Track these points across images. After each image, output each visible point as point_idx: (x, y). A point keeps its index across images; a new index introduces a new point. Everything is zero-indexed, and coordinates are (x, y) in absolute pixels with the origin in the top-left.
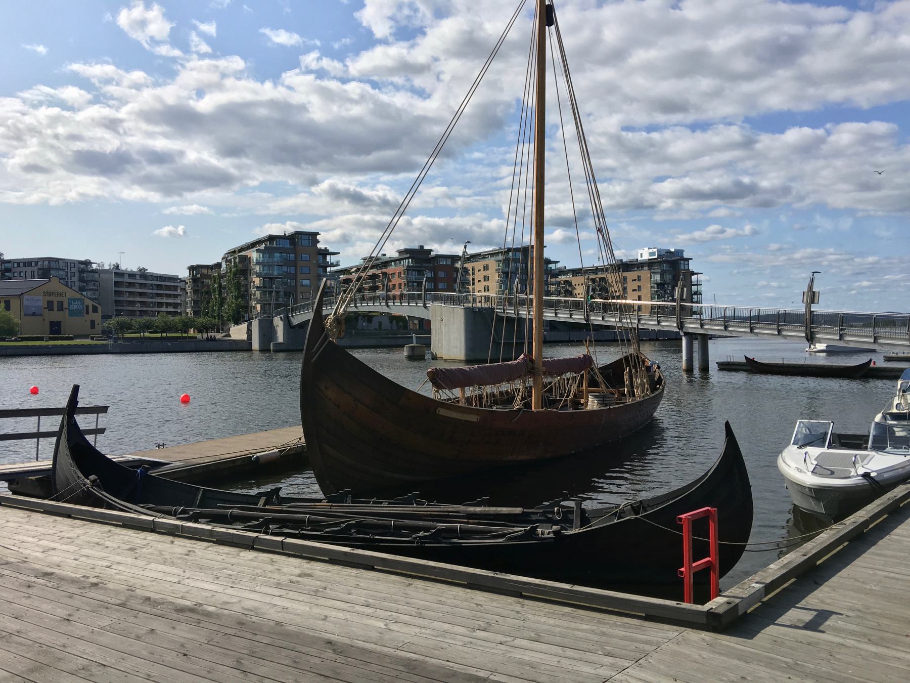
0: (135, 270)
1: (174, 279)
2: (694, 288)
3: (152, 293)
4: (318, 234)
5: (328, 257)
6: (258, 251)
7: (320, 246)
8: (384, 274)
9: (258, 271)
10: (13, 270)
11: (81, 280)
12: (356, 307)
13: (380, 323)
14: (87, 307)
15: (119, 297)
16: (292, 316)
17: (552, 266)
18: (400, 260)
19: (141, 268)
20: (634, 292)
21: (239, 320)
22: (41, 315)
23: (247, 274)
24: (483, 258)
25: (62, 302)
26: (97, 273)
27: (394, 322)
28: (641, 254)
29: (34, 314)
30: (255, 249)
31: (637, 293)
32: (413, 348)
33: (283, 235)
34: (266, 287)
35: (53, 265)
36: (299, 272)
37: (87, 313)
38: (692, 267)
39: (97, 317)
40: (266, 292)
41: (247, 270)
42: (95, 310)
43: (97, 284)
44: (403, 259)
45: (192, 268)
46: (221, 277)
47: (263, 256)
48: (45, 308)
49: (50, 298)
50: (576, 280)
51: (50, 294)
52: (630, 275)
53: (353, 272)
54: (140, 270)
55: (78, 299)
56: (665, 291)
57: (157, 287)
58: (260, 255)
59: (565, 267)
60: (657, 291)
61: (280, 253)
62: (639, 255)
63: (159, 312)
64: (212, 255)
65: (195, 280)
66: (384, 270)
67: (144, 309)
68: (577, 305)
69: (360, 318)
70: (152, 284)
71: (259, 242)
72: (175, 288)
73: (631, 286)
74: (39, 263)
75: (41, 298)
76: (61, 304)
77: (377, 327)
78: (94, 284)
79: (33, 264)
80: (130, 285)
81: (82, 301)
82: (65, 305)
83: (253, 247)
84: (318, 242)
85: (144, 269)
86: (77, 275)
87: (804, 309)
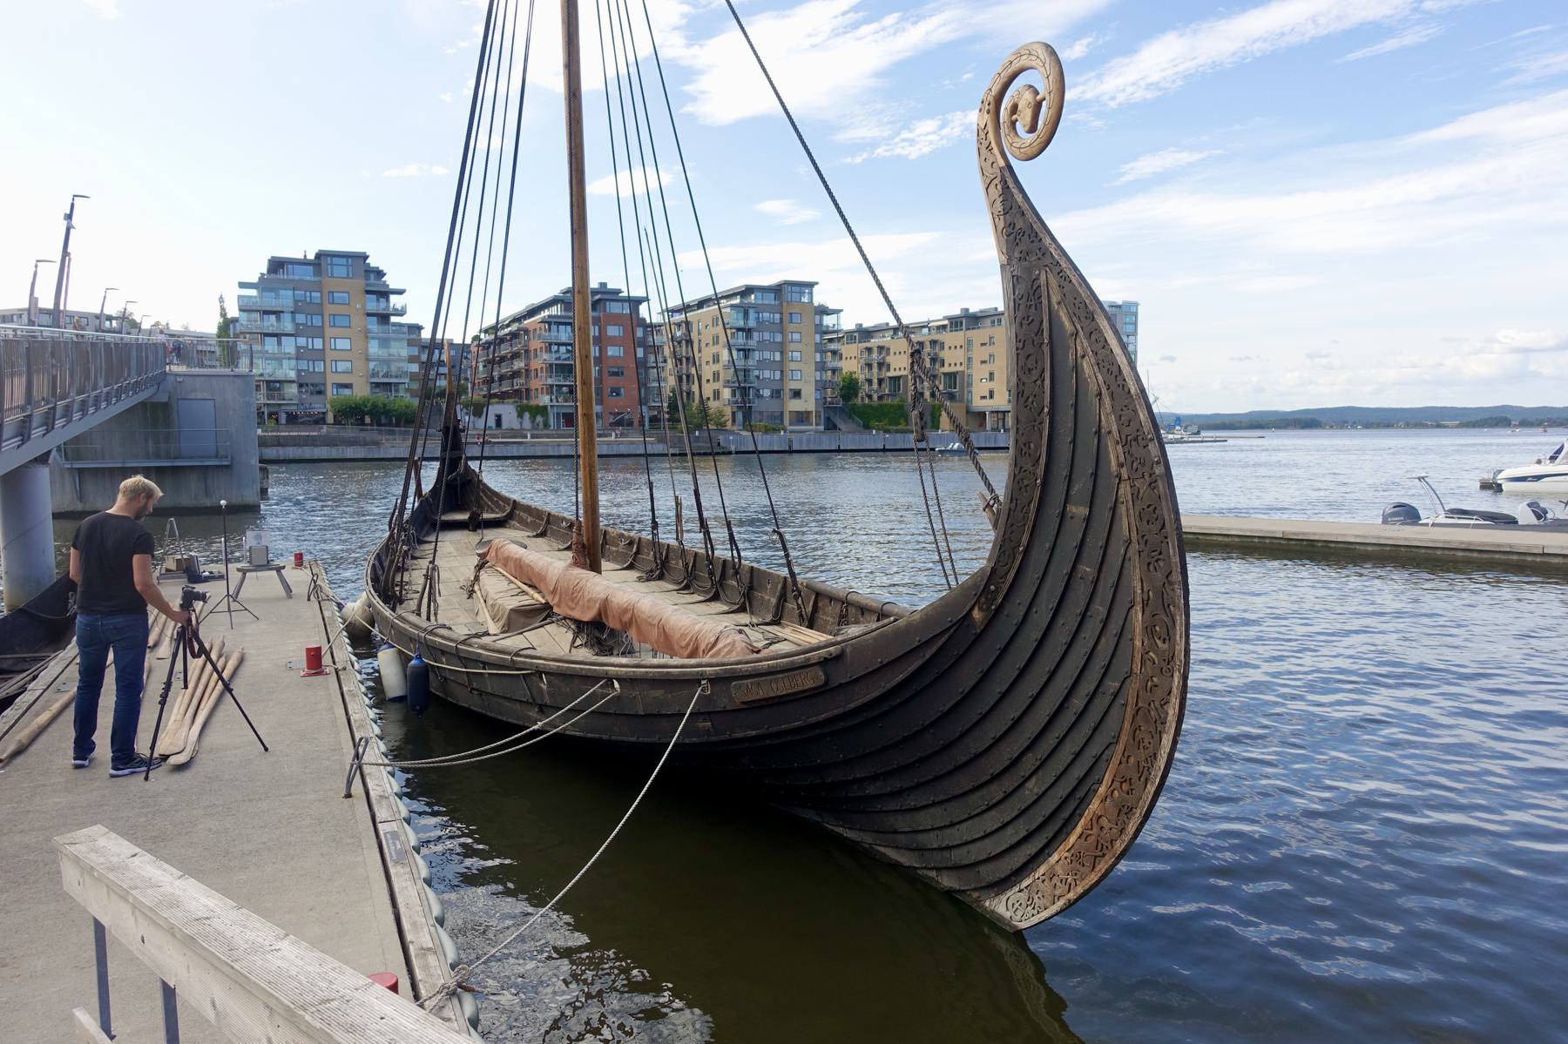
20: (984, 365)
27: (527, 415)
36: (327, 325)
52: (979, 335)
73: (979, 354)
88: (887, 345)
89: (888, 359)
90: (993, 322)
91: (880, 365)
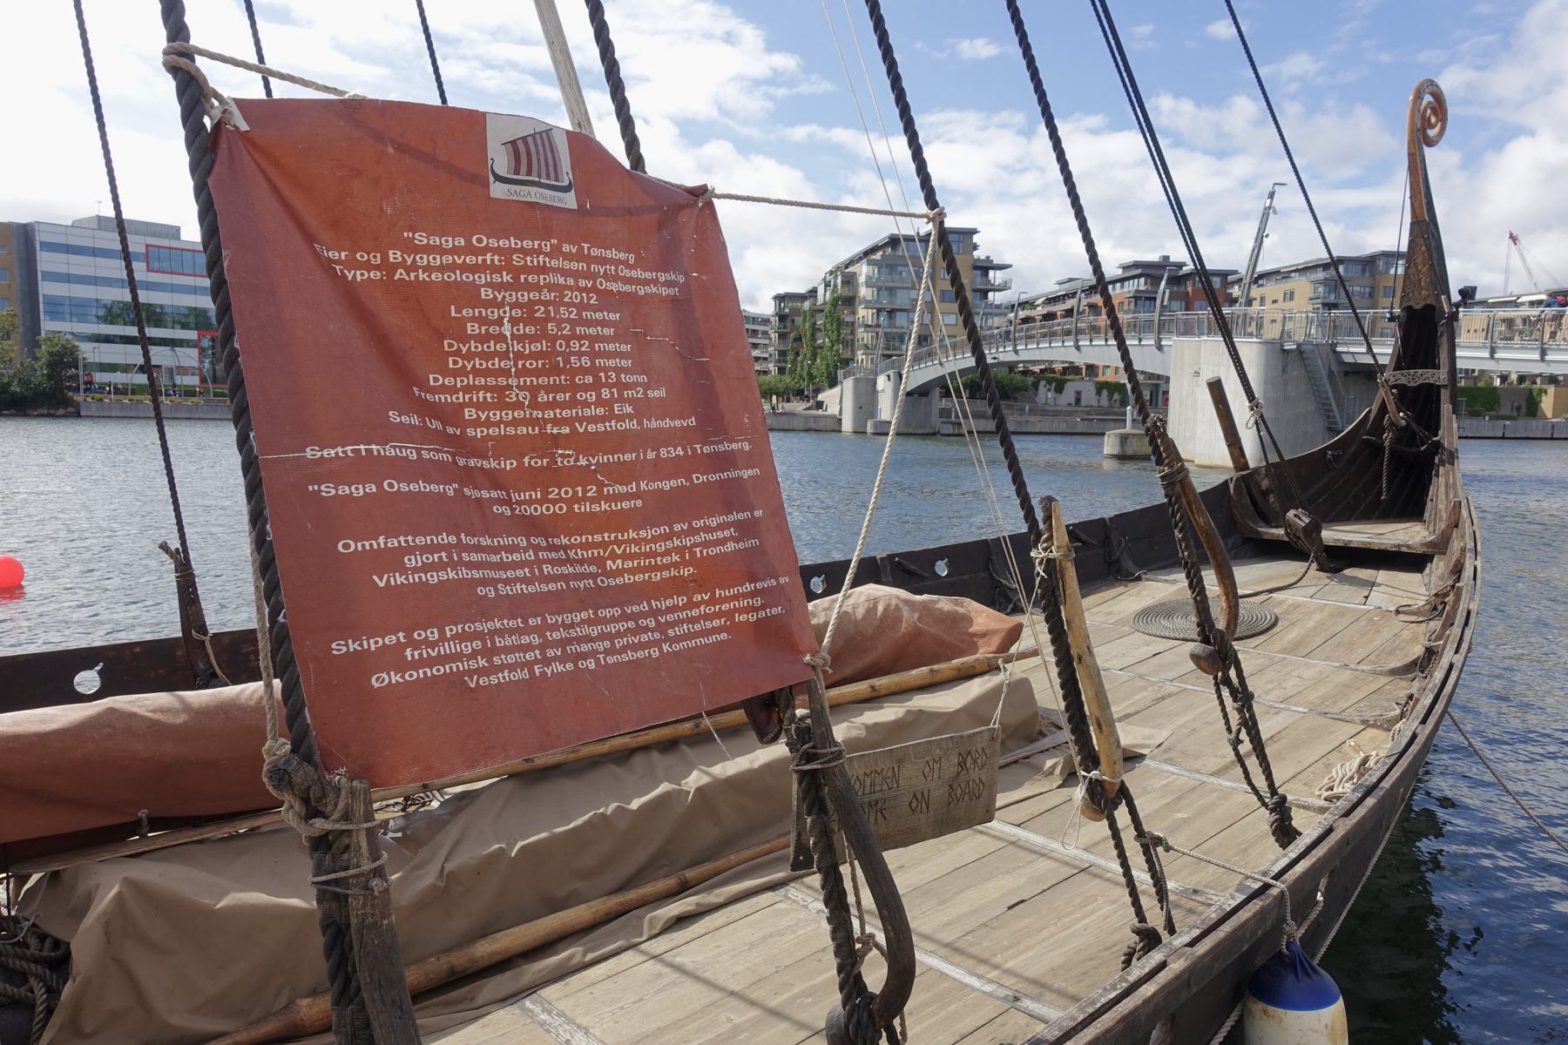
4: (974, 232)
5: (991, 273)
7: (979, 254)
13: (1079, 393)
24: (1283, 278)
27: (1105, 393)
32: (1124, 439)
44: (1128, 279)
46: (816, 311)
47: (879, 271)
53: (1038, 305)
69: (1043, 383)
71: (873, 250)
77: (1072, 401)
84: (975, 247)
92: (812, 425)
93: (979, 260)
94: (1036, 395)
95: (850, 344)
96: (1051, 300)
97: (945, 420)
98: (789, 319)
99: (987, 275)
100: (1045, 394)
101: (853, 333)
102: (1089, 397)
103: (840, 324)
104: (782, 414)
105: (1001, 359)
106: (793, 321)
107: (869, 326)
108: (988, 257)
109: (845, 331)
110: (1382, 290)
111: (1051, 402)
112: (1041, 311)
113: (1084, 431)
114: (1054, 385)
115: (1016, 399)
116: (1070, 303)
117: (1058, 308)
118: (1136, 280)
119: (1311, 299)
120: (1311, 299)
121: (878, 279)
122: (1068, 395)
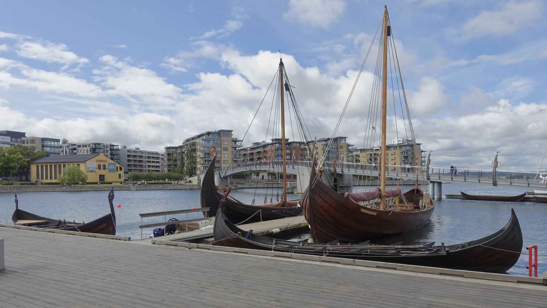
0: (134, 149)
1: (157, 154)
2: (423, 159)
3: (145, 161)
5: (237, 142)
6: (202, 140)
8: (265, 151)
9: (202, 150)
10: (78, 149)
11: (111, 154)
12: (256, 168)
13: (263, 177)
14: (117, 167)
15: (130, 162)
16: (222, 173)
17: (350, 148)
18: (272, 144)
19: (137, 148)
20: (392, 161)
21: (192, 175)
22: (95, 172)
23: (196, 151)
25: (105, 165)
26: (119, 150)
27: (270, 176)
28: (394, 141)
29: (92, 171)
30: (200, 138)
31: (394, 161)
33: (214, 131)
34: (206, 158)
35: (97, 146)
36: (222, 150)
37: (117, 171)
38: (422, 148)
39: (122, 173)
40: (206, 160)
41: (196, 149)
42: (121, 169)
43: (119, 156)
44: (274, 144)
45: (168, 148)
47: (205, 142)
48: (97, 168)
49: (99, 163)
50: (362, 155)
51: (100, 161)
54: (137, 149)
55: (113, 164)
56: (408, 160)
57: (148, 158)
58: (203, 142)
59: (356, 148)
60: (404, 161)
61: (213, 140)
62: (393, 142)
63: (149, 170)
64: (178, 142)
65: (169, 154)
66: (265, 149)
67: (141, 169)
68: (362, 167)
69: (253, 173)
70: (145, 156)
72: (157, 158)
74: (91, 146)
75: (95, 163)
76: (104, 166)
77: (261, 178)
78: (117, 156)
79: (88, 146)
80: (135, 156)
81: (115, 165)
82: (107, 167)
83: (199, 138)
84: (232, 135)
85: (138, 149)
86: (109, 151)
87: (492, 170)
88: (359, 154)
89: (360, 159)
90: (394, 148)
91: (357, 161)
92: (192, 187)
93: (233, 139)
94: (251, 177)
95: (195, 163)
96: (252, 149)
97: (232, 185)
98: (172, 155)
99: (236, 143)
100: (254, 177)
101: (196, 159)
102: (266, 177)
103: (193, 157)
104: (180, 185)
105: (252, 169)
106: (173, 155)
107: (202, 158)
108: (236, 138)
109: (194, 159)
110: (339, 147)
111: (255, 179)
112: (249, 152)
113: (263, 187)
114: (256, 174)
115: (246, 178)
116: (258, 150)
117: (254, 151)
118: (277, 144)
119: (322, 149)
120: (322, 149)
121: (205, 144)
122: (260, 177)
